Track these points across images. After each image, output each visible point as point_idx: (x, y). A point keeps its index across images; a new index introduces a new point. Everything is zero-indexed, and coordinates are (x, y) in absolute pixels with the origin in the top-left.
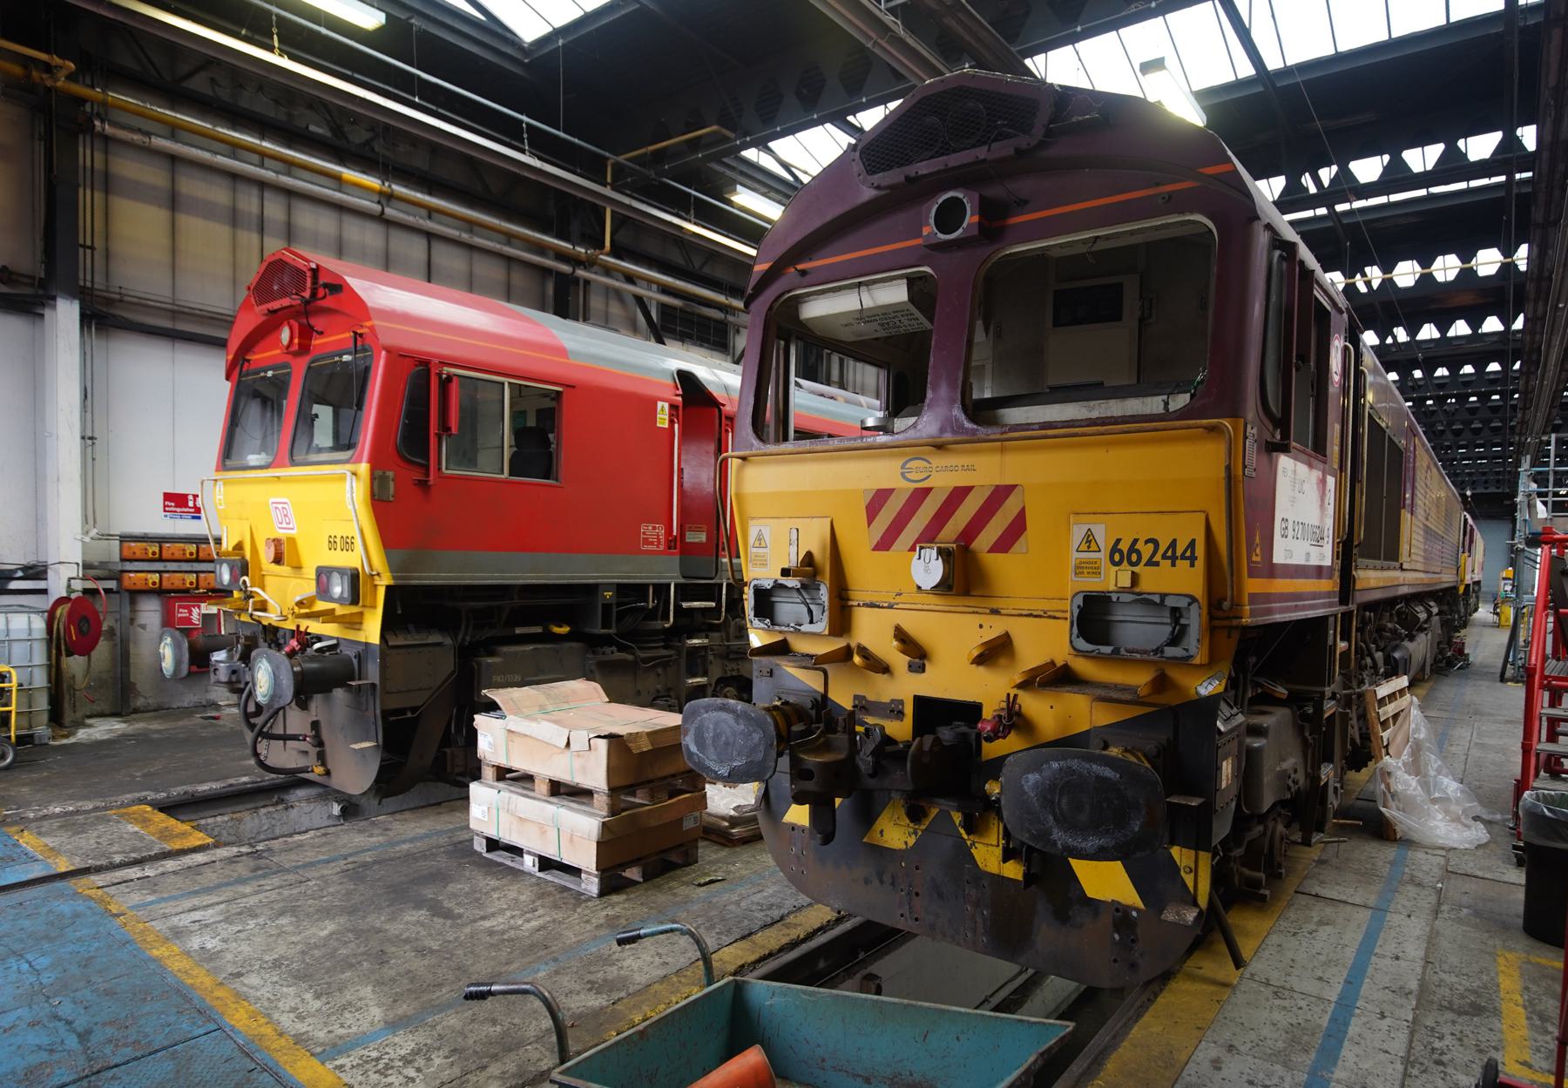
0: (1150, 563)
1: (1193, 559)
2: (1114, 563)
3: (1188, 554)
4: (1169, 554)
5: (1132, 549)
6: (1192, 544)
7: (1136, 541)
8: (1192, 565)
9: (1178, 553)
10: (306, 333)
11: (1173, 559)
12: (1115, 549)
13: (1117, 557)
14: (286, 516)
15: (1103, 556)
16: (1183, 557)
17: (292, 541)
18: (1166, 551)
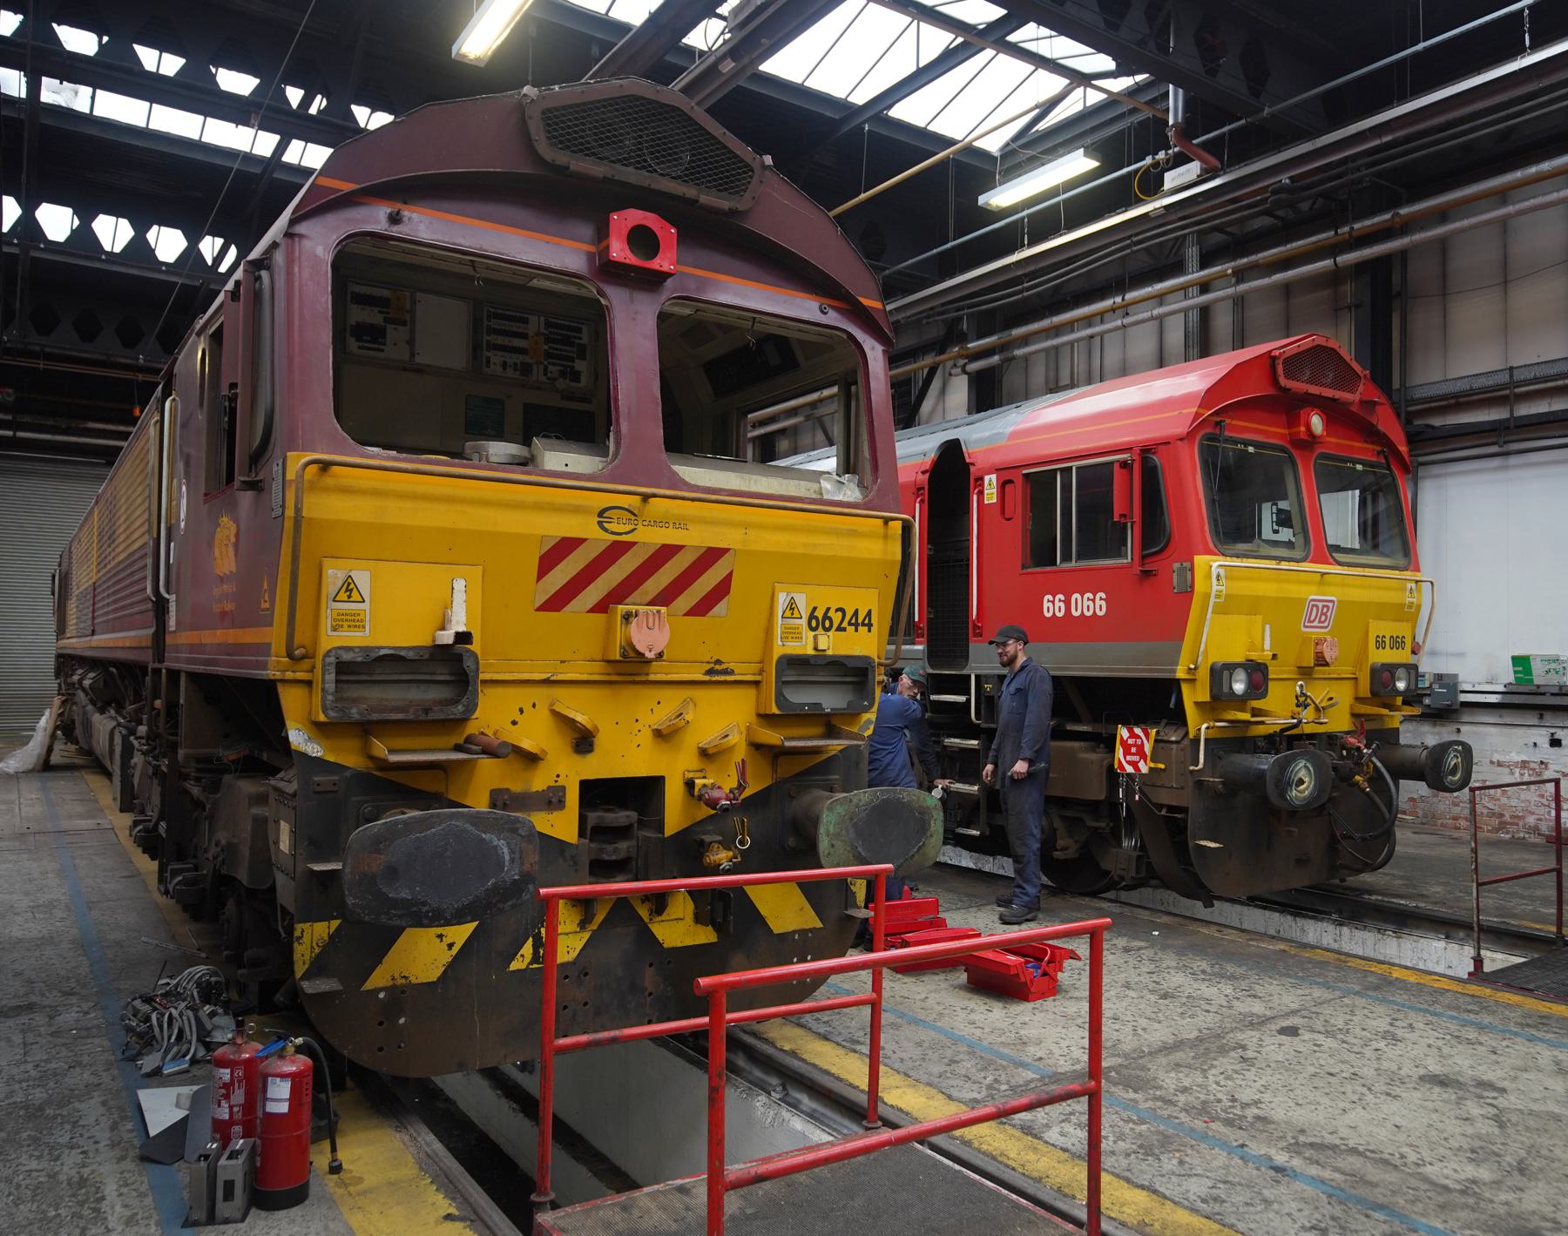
0: (840, 629)
1: (870, 625)
2: (813, 629)
3: (867, 621)
4: (853, 621)
5: (826, 617)
6: (869, 614)
7: (828, 609)
8: (869, 631)
9: (860, 621)
11: (856, 625)
12: (812, 616)
13: (814, 623)
14: (1325, 614)
15: (804, 621)
16: (863, 624)
18: (864, 620)
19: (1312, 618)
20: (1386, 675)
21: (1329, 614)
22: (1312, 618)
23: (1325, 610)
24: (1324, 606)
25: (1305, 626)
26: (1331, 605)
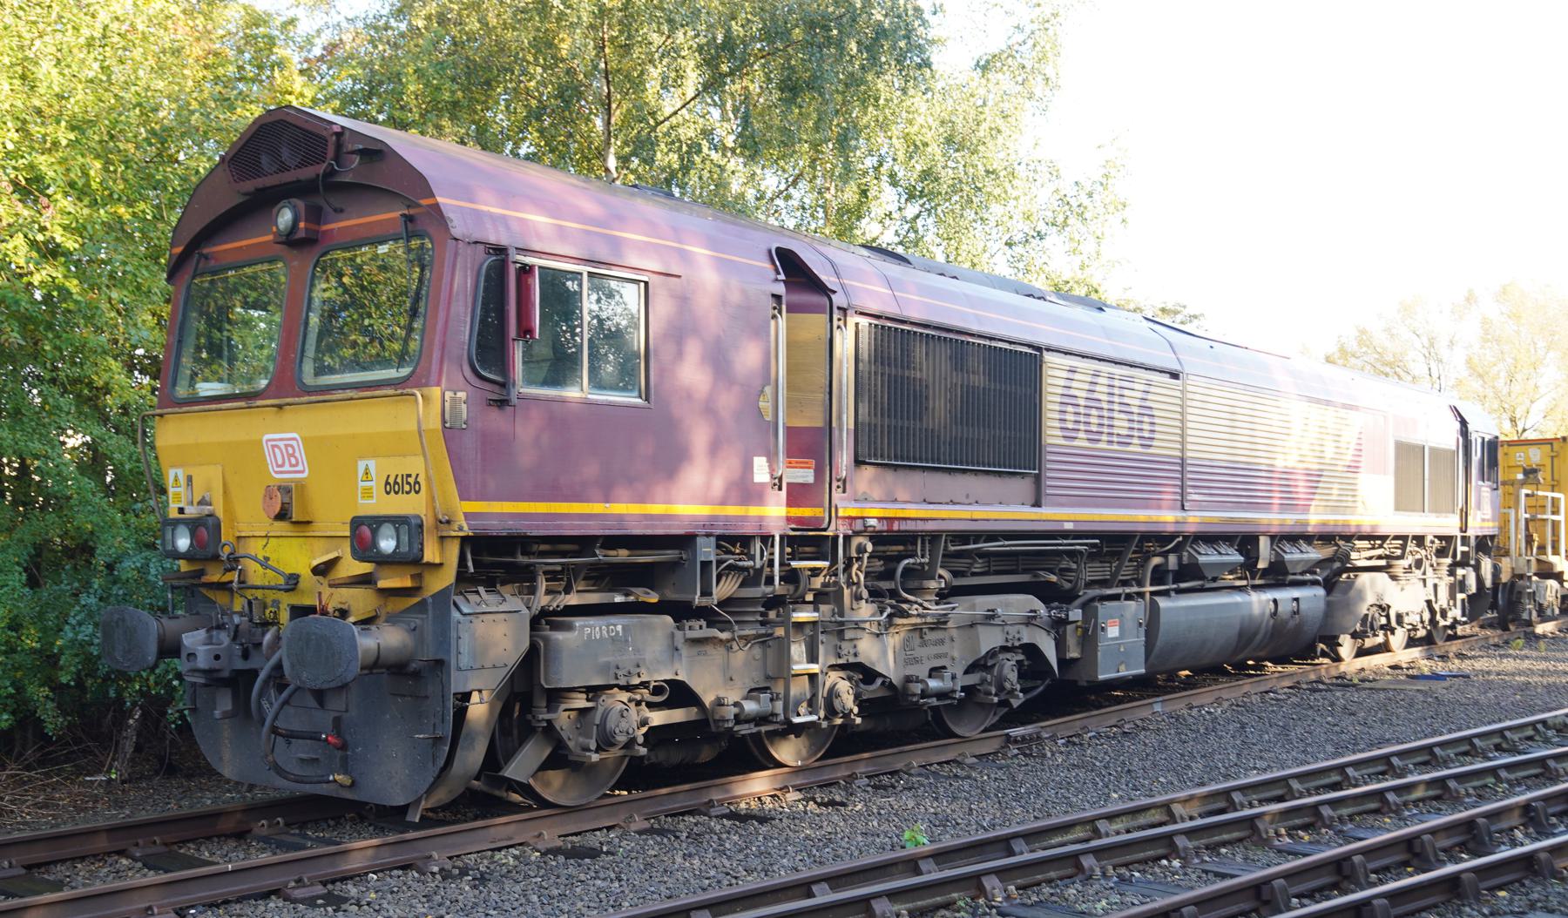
10: (315, 215)
14: (293, 455)
17: (301, 485)
19: (280, 462)
20: (366, 530)
21: (297, 454)
22: (280, 462)
23: (290, 451)
24: (286, 446)
25: (276, 472)
26: (294, 443)
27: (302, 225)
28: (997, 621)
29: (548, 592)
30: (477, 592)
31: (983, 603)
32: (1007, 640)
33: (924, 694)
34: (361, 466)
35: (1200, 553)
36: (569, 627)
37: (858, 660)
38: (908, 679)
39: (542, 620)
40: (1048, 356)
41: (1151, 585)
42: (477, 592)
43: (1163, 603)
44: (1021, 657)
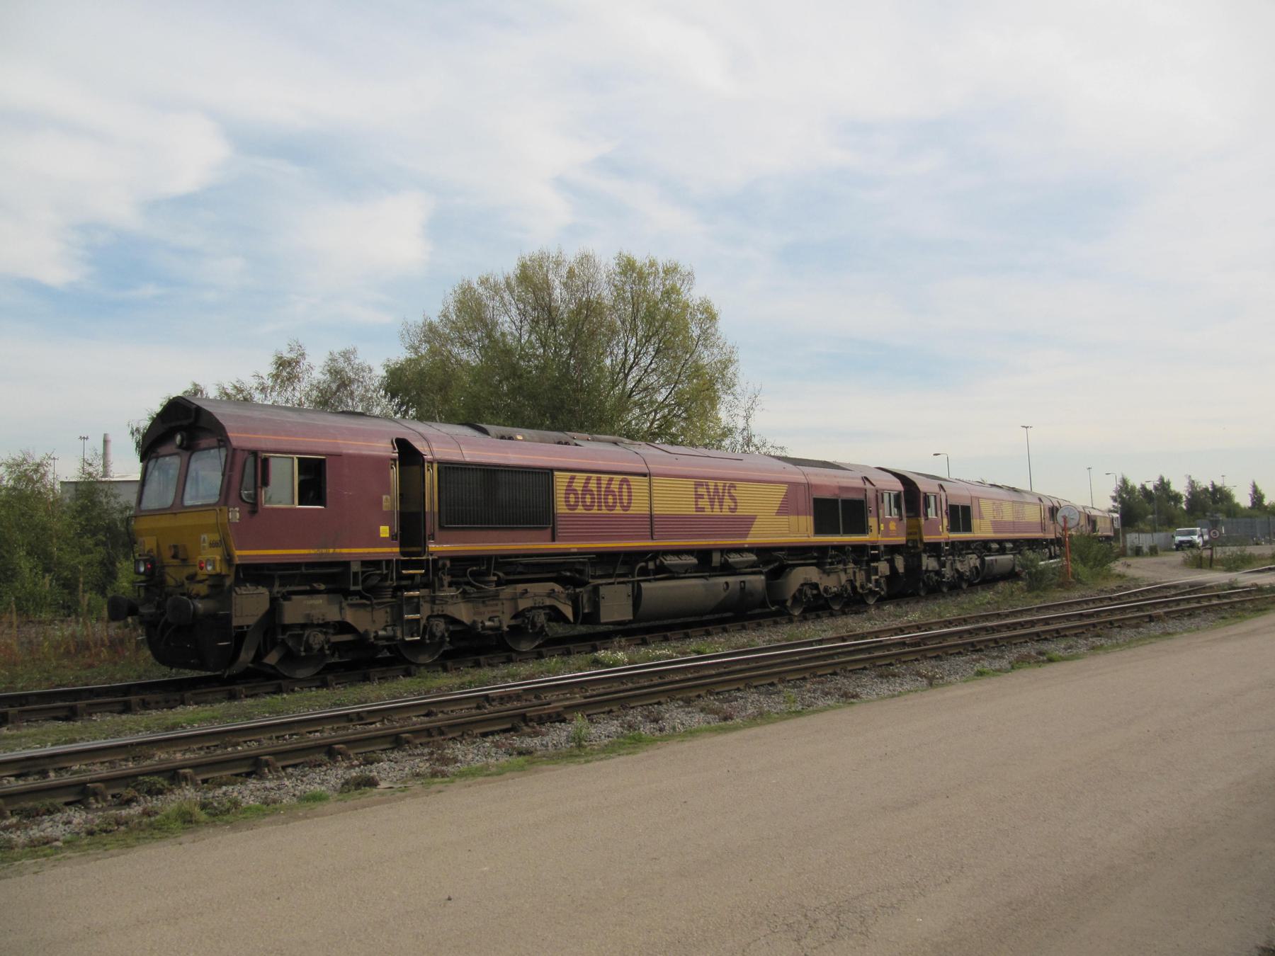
27: (185, 442)
28: (528, 595)
29: (280, 586)
30: (246, 586)
31: (520, 587)
32: (535, 604)
33: (484, 627)
34: (203, 537)
35: (666, 560)
36: (289, 599)
37: (444, 613)
38: (474, 622)
39: (273, 600)
40: (556, 473)
41: (638, 576)
42: (246, 586)
43: (643, 585)
44: (547, 611)
